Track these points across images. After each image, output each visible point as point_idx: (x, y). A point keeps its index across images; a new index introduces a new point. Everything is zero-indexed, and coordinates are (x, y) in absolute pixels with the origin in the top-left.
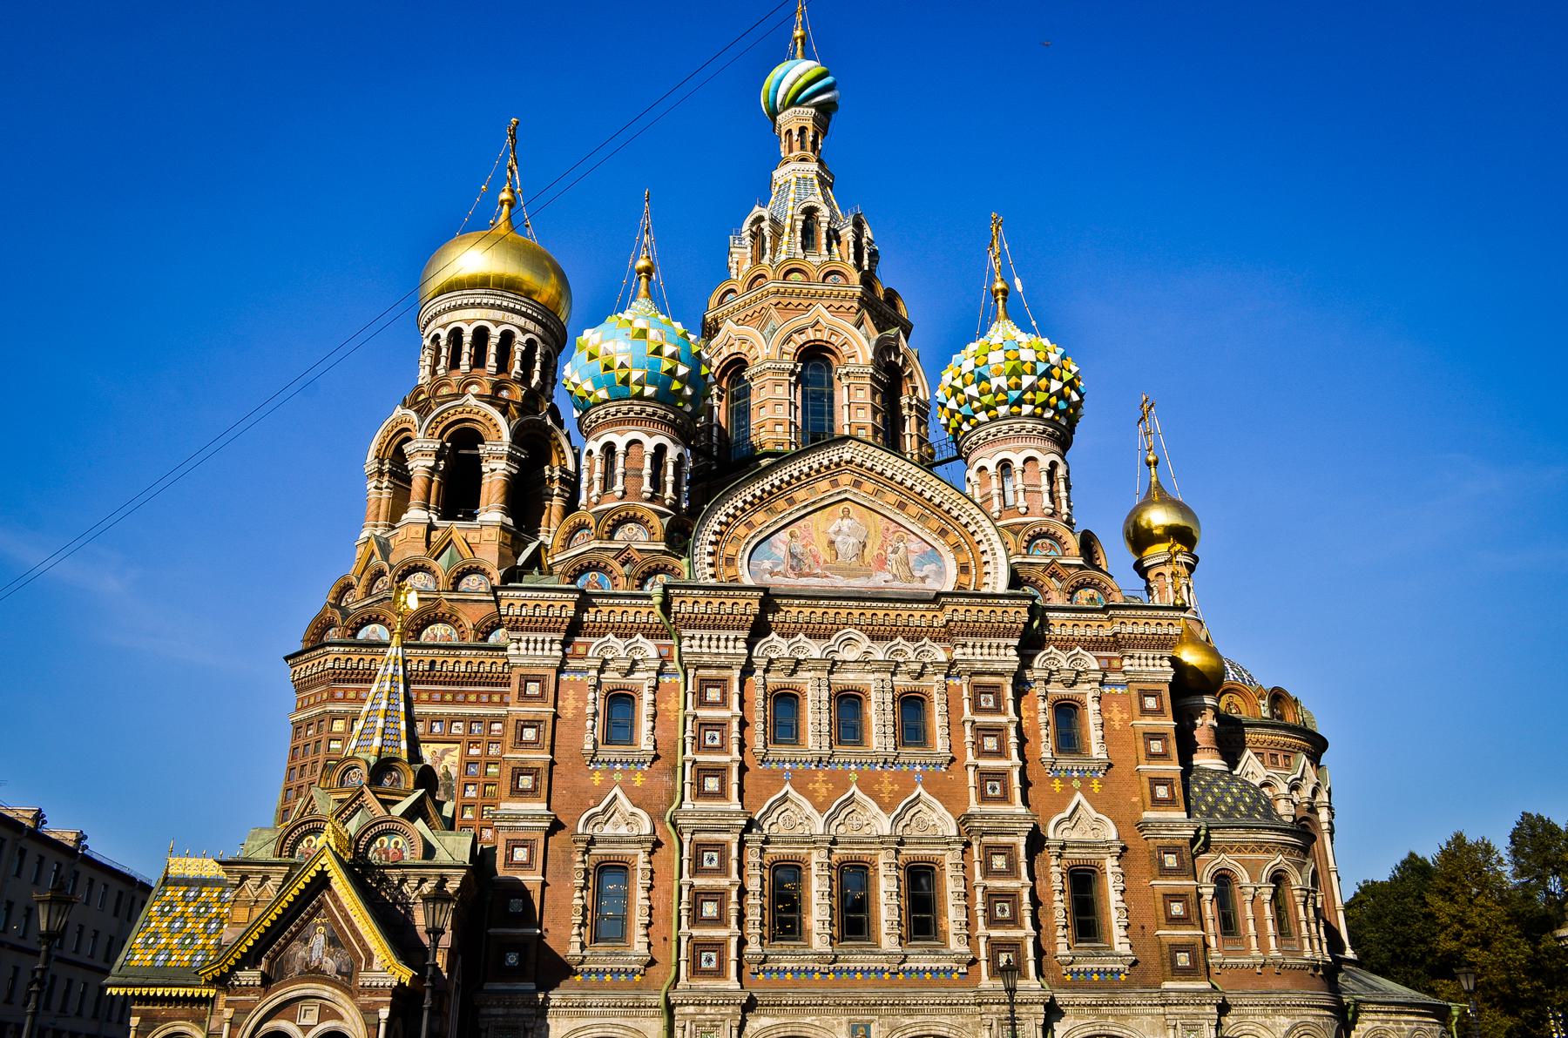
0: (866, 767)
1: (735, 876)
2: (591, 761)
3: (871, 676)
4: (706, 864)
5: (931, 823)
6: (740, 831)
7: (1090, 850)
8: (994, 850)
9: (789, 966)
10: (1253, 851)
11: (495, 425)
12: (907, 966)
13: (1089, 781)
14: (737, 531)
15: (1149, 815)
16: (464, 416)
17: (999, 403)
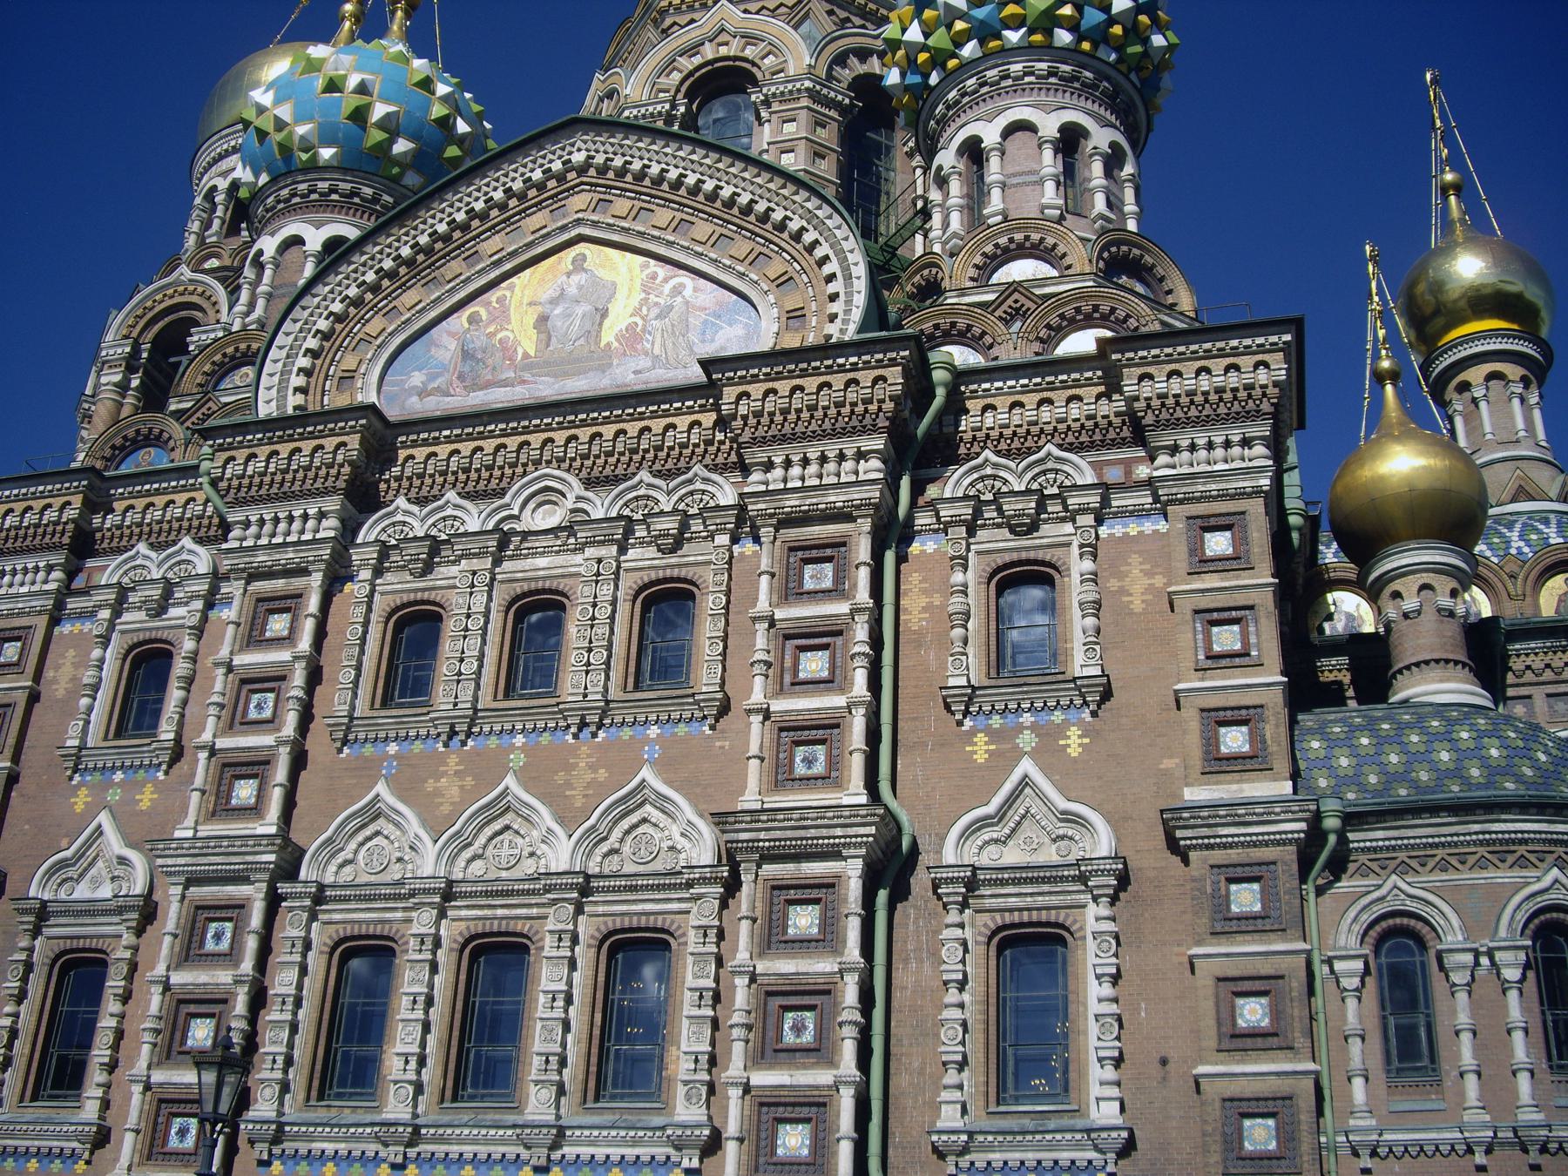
0: (546, 738)
1: (247, 966)
2: (76, 770)
3: (578, 558)
4: (210, 946)
5: (665, 845)
6: (266, 876)
7: (1046, 888)
8: (792, 894)
9: (329, 1147)
10: (1481, 864)
11: (215, 304)
12: (569, 1151)
13: (1061, 730)
14: (367, 329)
15: (1195, 794)
16: (178, 299)
17: (959, 44)
